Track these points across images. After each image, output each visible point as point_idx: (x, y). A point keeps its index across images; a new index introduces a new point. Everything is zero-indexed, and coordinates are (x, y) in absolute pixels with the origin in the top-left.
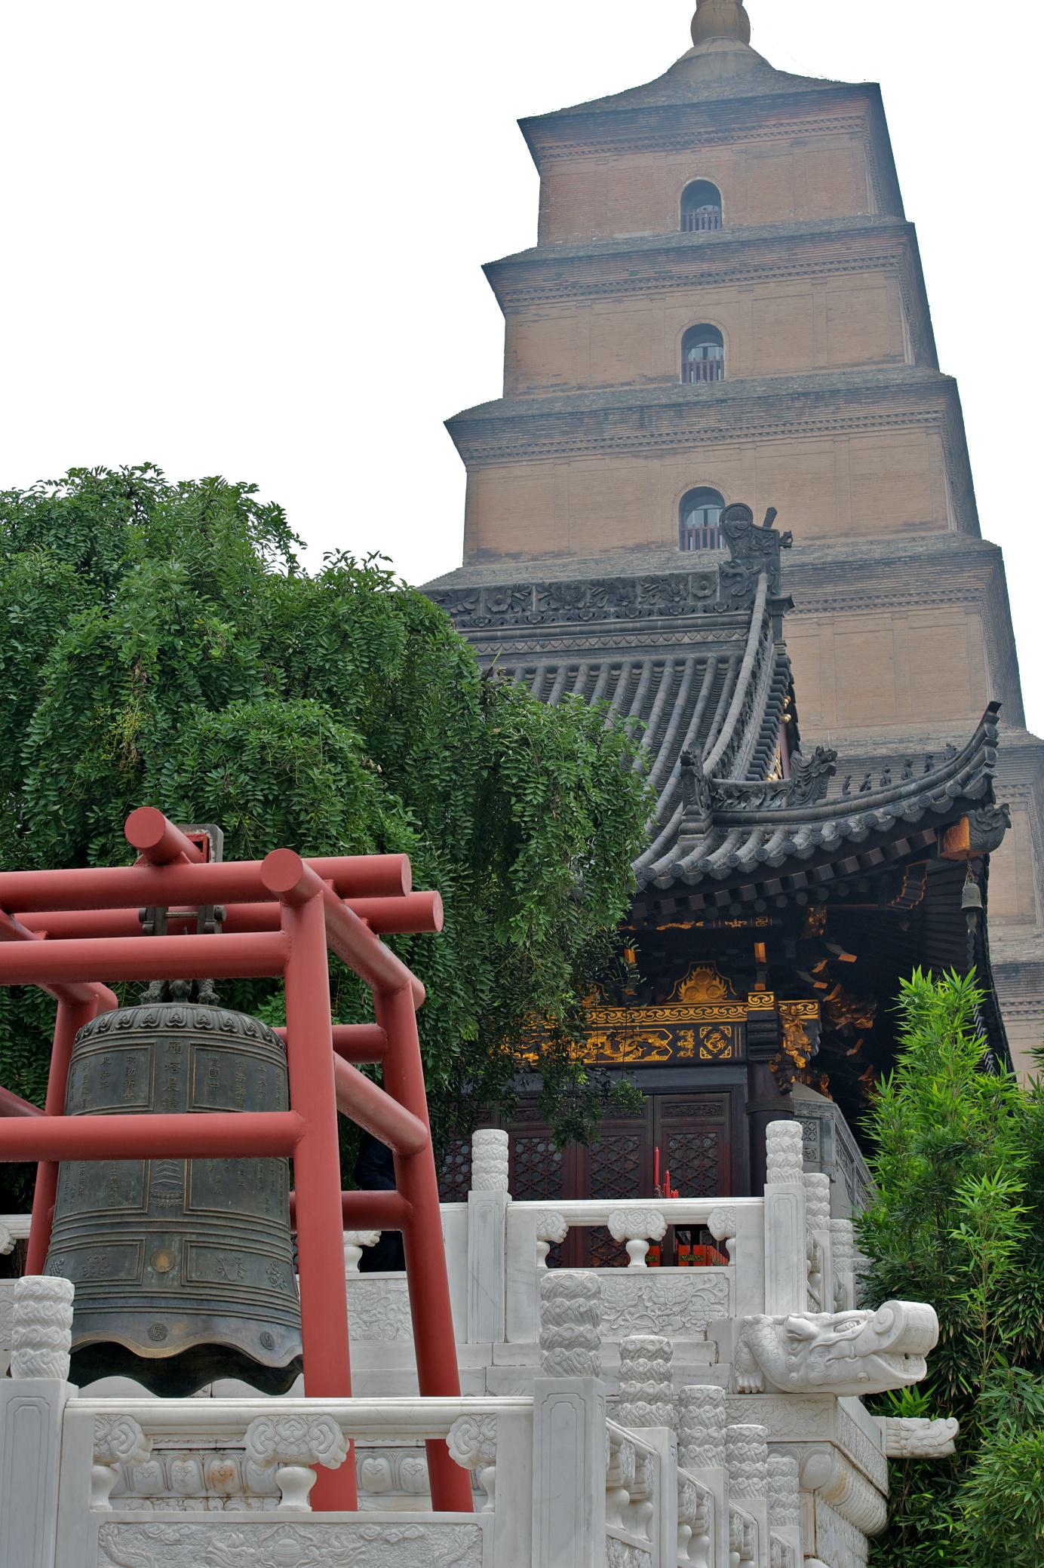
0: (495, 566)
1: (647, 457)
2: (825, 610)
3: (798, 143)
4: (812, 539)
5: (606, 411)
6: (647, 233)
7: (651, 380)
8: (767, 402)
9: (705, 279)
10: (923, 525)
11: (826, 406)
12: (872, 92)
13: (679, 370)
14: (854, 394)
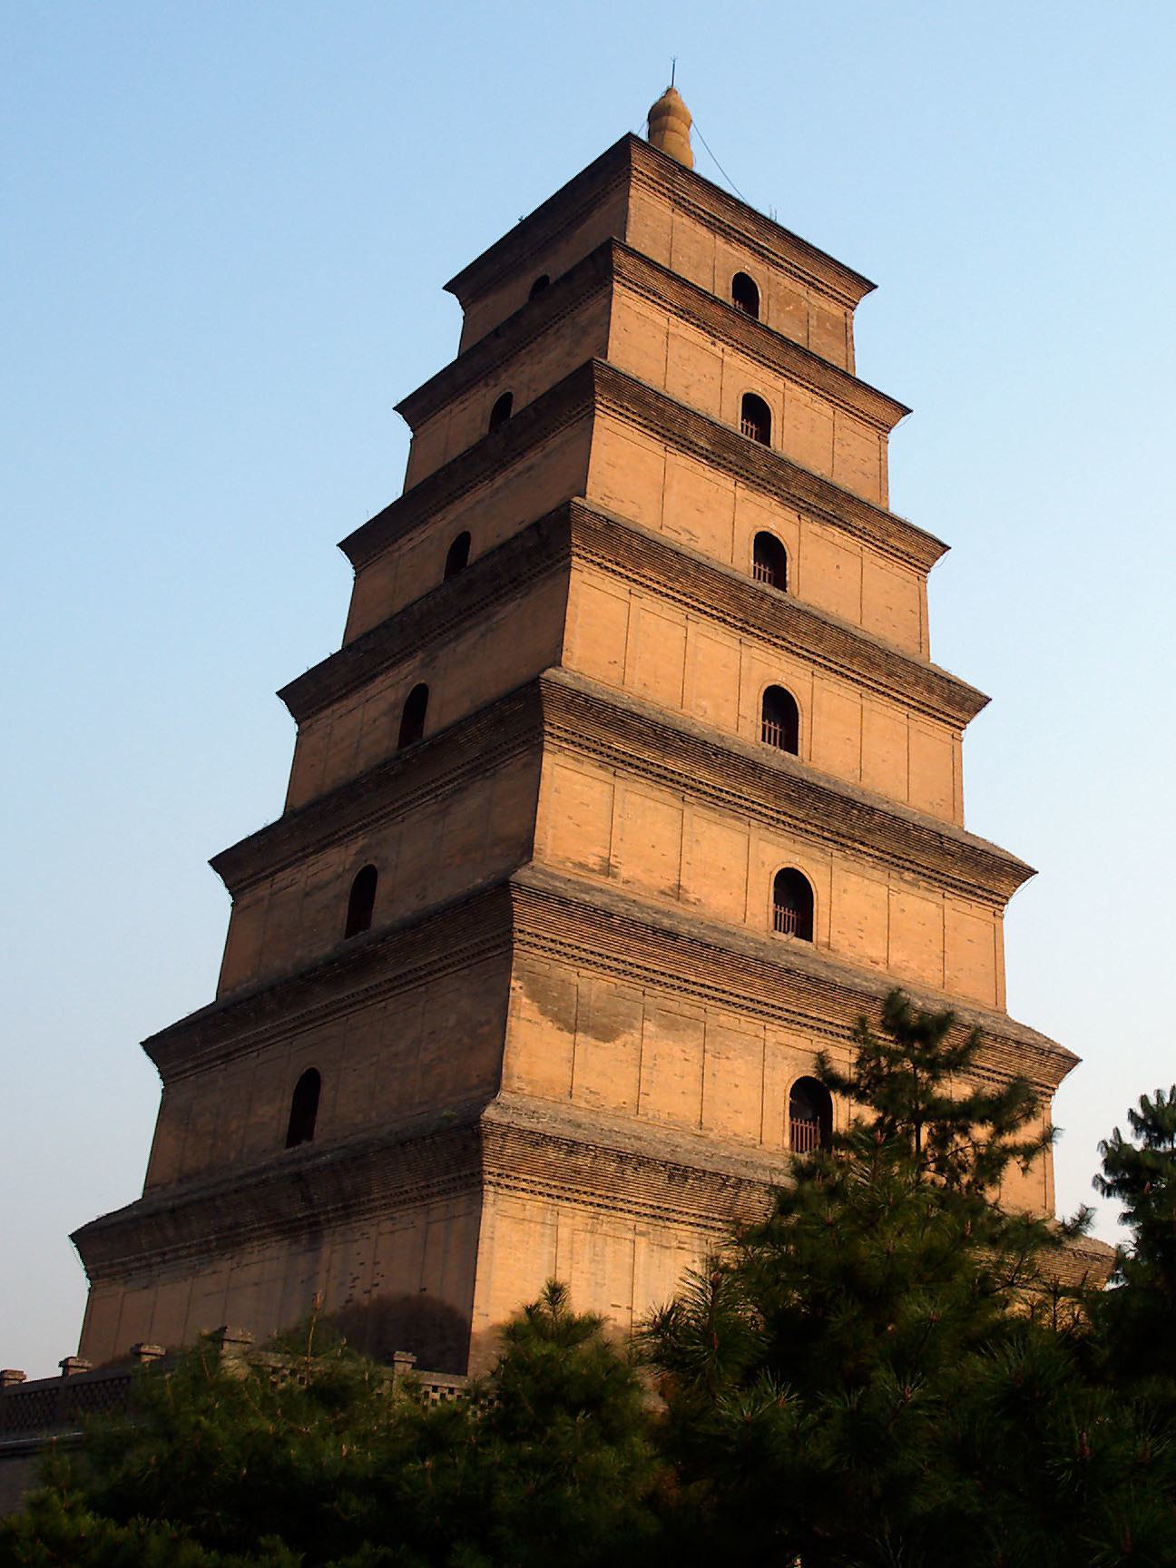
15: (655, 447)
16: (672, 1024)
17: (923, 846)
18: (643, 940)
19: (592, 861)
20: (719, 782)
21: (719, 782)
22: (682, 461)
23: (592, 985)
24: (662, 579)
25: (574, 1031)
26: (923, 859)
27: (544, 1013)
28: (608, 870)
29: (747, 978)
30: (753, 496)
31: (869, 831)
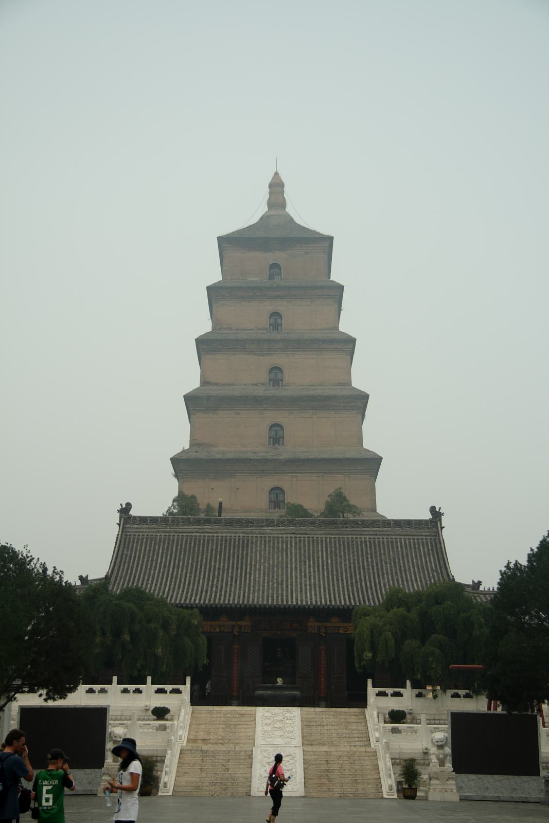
0: (211, 387)
1: (259, 356)
2: (314, 410)
3: (306, 253)
4: (310, 386)
5: (247, 340)
6: (258, 279)
7: (259, 329)
9: (277, 297)
10: (344, 384)
11: (316, 344)
12: (330, 239)
13: (268, 326)
14: (324, 341)
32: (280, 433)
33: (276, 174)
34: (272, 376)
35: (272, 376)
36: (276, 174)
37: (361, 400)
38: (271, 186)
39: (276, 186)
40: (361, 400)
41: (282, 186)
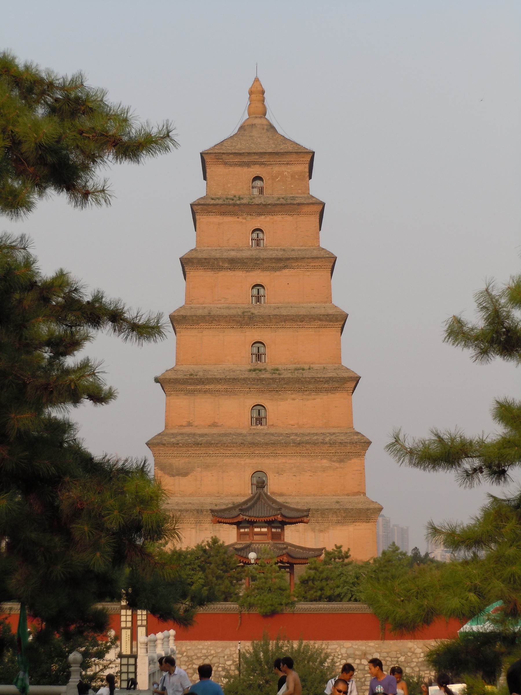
8: (279, 260)
15: (210, 273)
16: (207, 467)
17: (309, 383)
18: (191, 447)
19: (184, 423)
20: (225, 387)
21: (225, 387)
22: (221, 274)
23: (178, 462)
24: (207, 324)
25: (173, 476)
26: (311, 386)
27: (165, 473)
28: (189, 424)
29: (229, 448)
30: (252, 274)
31: (285, 384)
32: (262, 350)
33: (257, 80)
34: (255, 291)
35: (255, 291)
36: (257, 80)
37: (340, 320)
38: (251, 93)
39: (257, 93)
40: (340, 320)
41: (263, 92)
